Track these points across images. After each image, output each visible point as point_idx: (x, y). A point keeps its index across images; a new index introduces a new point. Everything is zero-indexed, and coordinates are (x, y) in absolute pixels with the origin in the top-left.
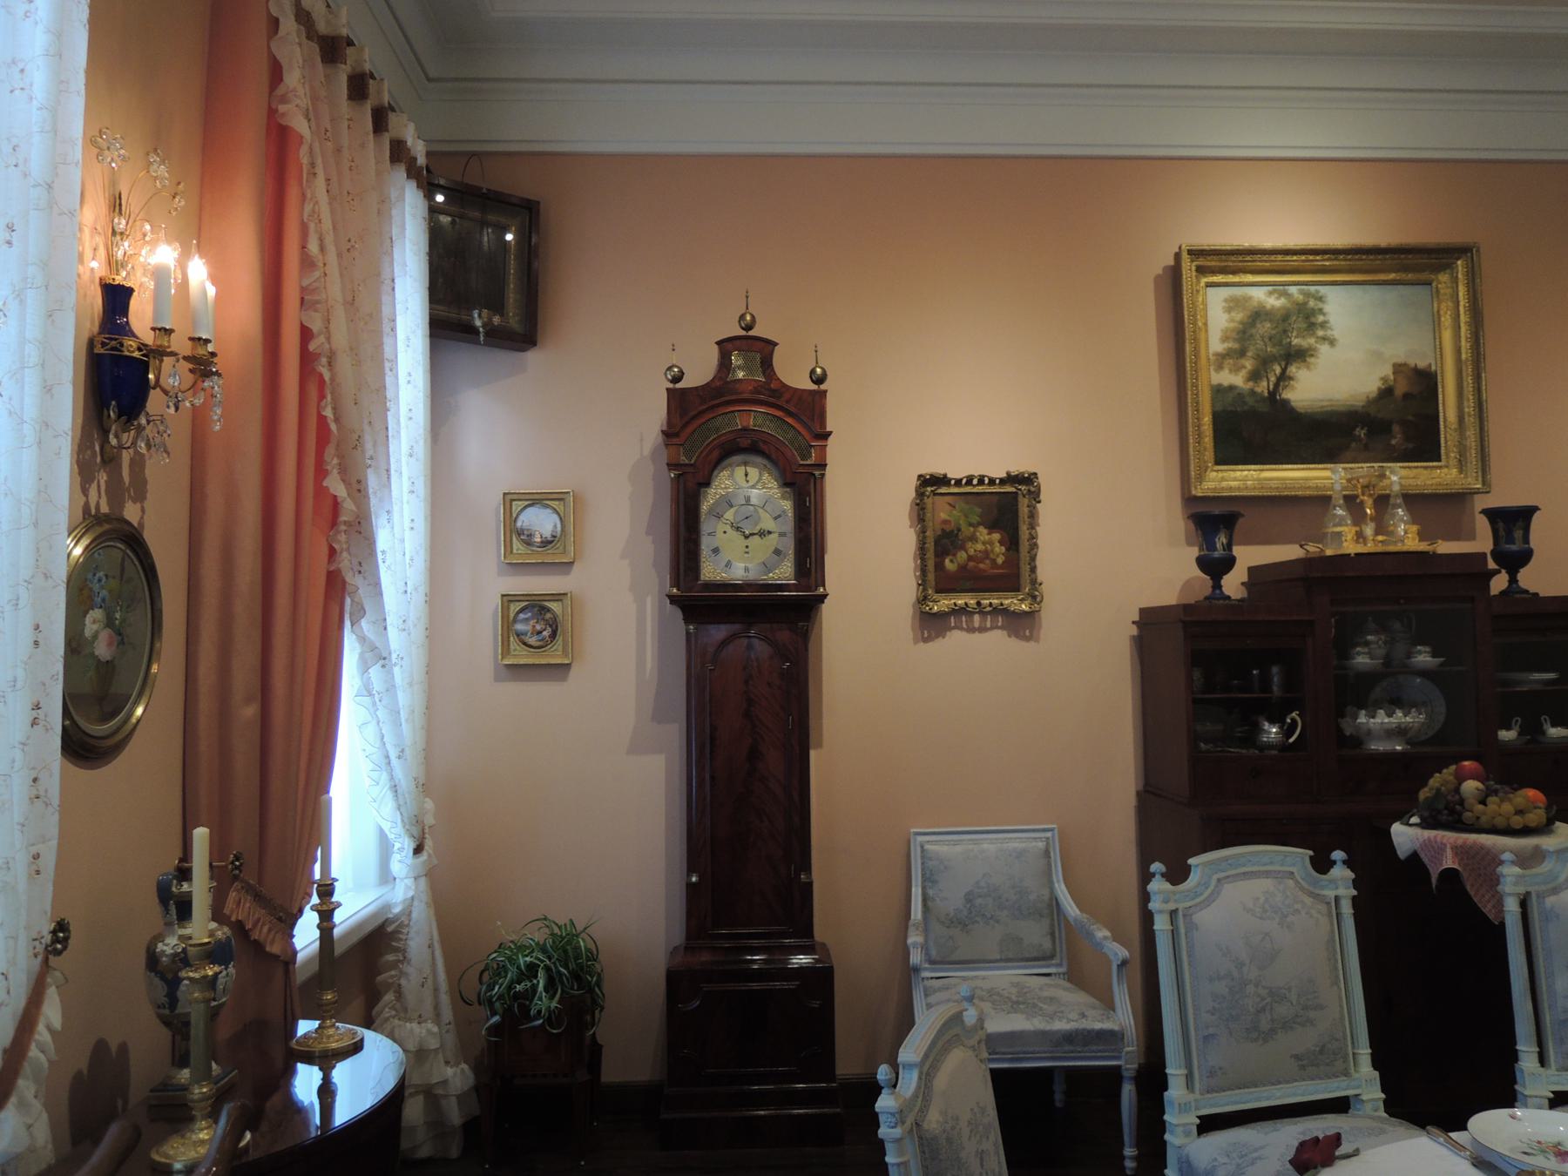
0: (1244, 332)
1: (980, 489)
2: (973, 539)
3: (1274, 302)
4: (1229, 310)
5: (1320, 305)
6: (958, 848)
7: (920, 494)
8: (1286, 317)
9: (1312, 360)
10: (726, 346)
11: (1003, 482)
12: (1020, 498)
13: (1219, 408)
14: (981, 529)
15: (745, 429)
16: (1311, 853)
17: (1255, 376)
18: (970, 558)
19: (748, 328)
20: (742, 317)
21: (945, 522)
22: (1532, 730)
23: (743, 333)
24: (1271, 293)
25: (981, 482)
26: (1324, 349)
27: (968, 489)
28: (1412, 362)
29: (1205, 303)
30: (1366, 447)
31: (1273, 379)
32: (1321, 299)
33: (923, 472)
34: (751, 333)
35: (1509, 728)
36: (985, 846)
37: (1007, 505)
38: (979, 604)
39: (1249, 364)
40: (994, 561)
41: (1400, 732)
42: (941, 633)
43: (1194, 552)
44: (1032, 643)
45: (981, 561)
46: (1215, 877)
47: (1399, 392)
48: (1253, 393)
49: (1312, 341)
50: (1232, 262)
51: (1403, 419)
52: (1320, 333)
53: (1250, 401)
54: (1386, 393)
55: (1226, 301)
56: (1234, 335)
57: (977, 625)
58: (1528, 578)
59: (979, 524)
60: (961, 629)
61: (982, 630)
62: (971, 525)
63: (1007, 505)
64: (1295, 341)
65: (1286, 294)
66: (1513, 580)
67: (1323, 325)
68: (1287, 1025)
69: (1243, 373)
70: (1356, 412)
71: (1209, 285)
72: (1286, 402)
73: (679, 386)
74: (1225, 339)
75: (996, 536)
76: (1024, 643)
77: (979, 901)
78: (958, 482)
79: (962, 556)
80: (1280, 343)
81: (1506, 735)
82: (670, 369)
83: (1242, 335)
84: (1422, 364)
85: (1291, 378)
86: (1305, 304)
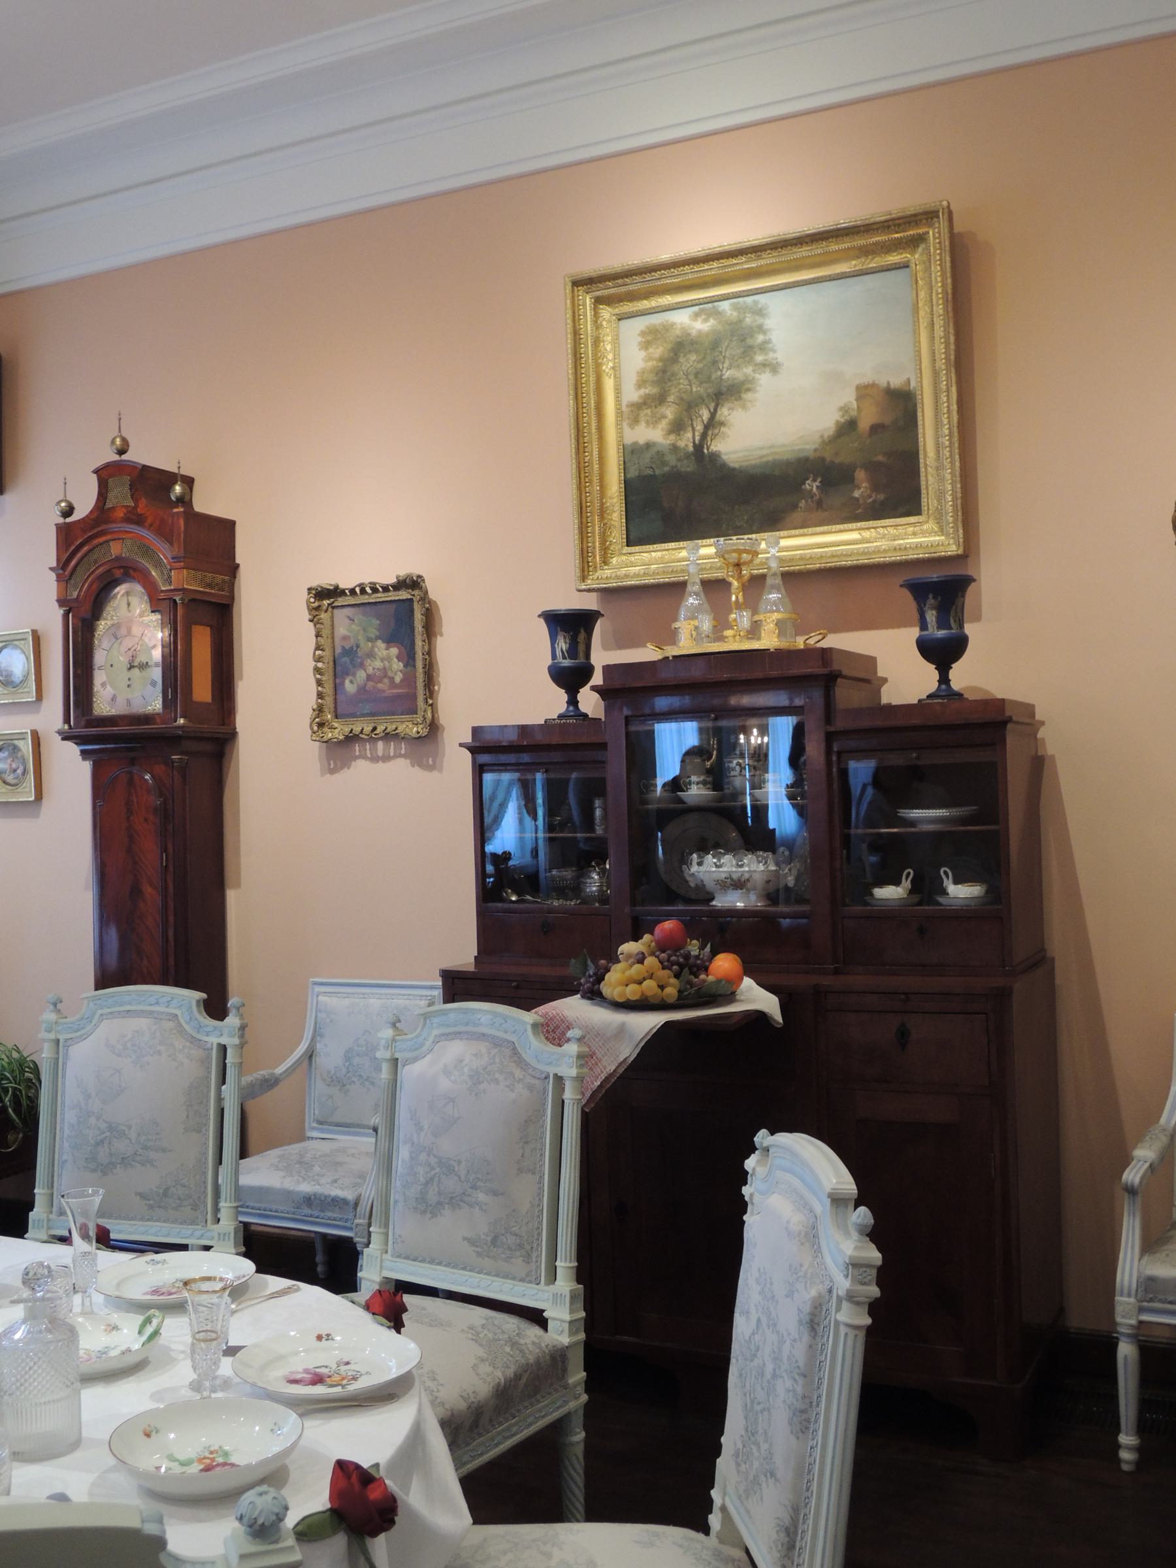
0: (664, 372)
1: (373, 599)
2: (371, 655)
3: (701, 326)
4: (646, 345)
5: (760, 320)
6: (347, 1002)
7: (315, 611)
8: (715, 345)
9: (748, 396)
10: (105, 474)
11: (401, 585)
12: (415, 604)
13: (633, 473)
14: (381, 645)
15: (118, 558)
16: (204, 996)
17: (677, 427)
18: (369, 678)
19: (121, 452)
20: (113, 442)
21: (345, 638)
22: (926, 888)
23: (117, 458)
24: (696, 315)
25: (375, 590)
26: (765, 379)
27: (365, 599)
28: (882, 381)
29: (616, 341)
30: (819, 504)
31: (699, 428)
32: (760, 312)
33: (314, 584)
34: (124, 457)
35: (897, 882)
36: (372, 1001)
37: (404, 613)
38: (375, 729)
39: (670, 412)
40: (392, 679)
41: (738, 884)
42: (345, 763)
43: (549, 662)
44: (435, 773)
45: (380, 681)
46: (100, 1012)
47: (864, 424)
48: (675, 448)
49: (748, 370)
50: (635, 285)
51: (874, 464)
52: (759, 358)
53: (672, 460)
54: (848, 427)
55: (643, 333)
56: (652, 377)
57: (380, 753)
58: (962, 676)
59: (377, 638)
60: (365, 757)
61: (386, 758)
62: (369, 640)
63: (404, 613)
64: (727, 374)
65: (717, 313)
66: (944, 679)
67: (764, 347)
68: (125, 1162)
69: (664, 424)
70: (807, 459)
71: (621, 318)
72: (714, 457)
73: (68, 520)
74: (641, 384)
75: (394, 651)
76: (426, 773)
77: (356, 1060)
78: (353, 591)
79: (361, 675)
80: (709, 379)
81: (889, 893)
82: (59, 503)
83: (662, 375)
84: (896, 382)
85: (722, 424)
86: (740, 321)
